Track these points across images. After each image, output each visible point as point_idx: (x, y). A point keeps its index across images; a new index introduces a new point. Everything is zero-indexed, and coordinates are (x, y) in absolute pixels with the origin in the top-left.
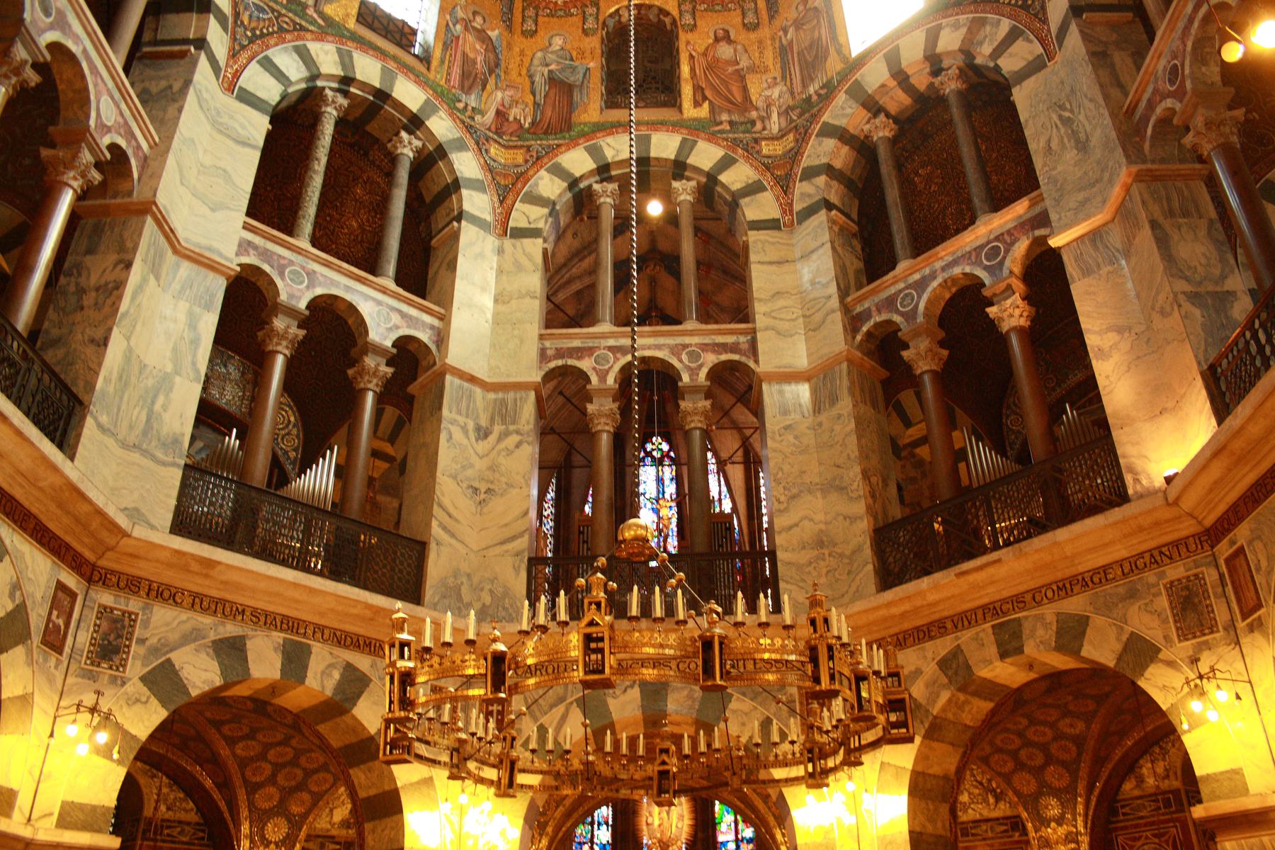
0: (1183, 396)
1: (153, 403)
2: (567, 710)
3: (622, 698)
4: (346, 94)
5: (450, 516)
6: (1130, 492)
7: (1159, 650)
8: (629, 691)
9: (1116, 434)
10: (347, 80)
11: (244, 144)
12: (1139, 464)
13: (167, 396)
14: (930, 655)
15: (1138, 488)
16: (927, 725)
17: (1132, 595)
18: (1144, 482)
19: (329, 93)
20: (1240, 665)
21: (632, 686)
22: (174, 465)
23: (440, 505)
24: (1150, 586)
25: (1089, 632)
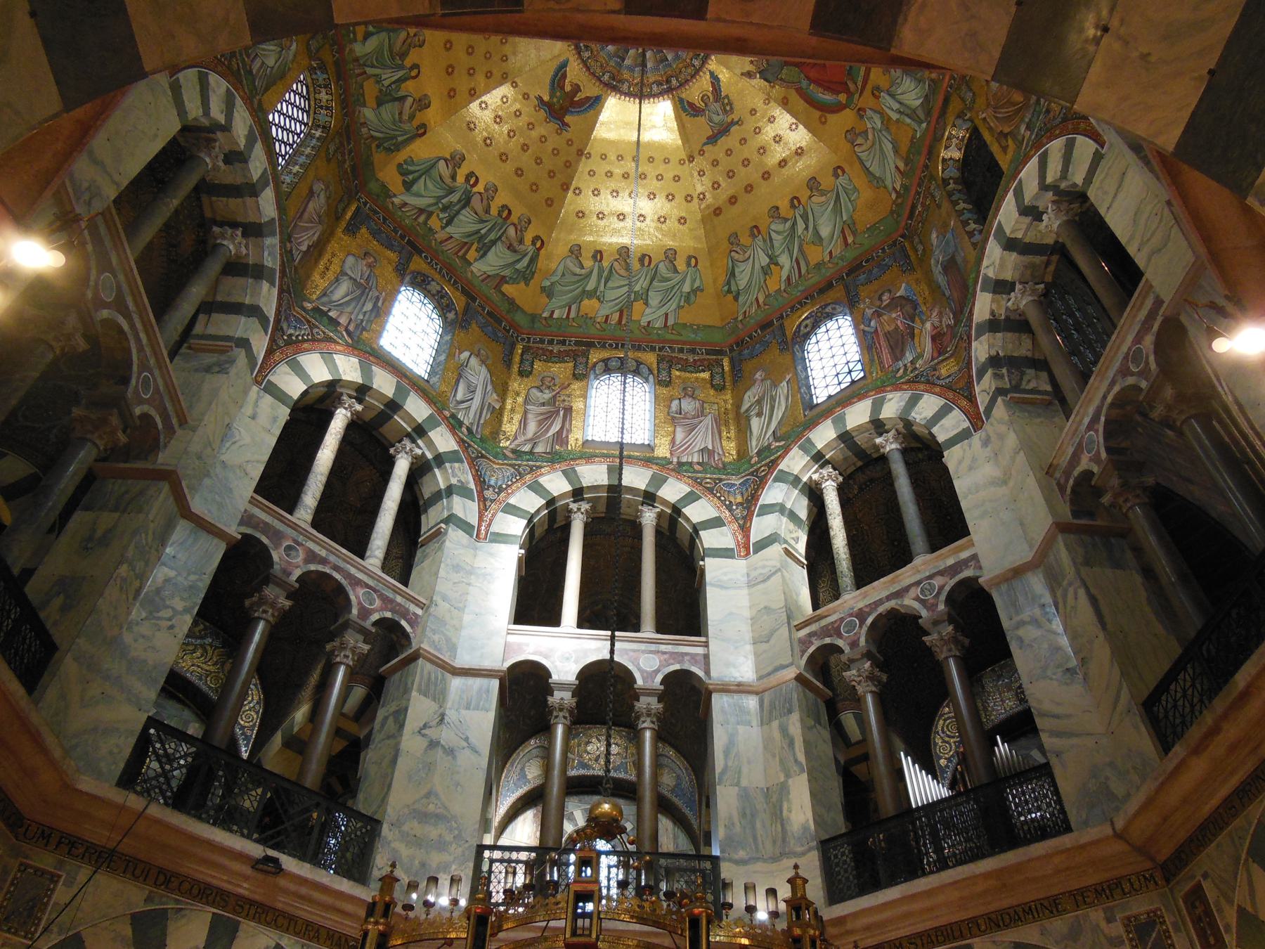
1: (781, 812)
2: (1248, 871)
4: (827, 462)
5: (1057, 717)
10: (819, 458)
11: (769, 578)
13: (788, 800)
19: (815, 477)
22: (810, 850)
23: (1044, 715)
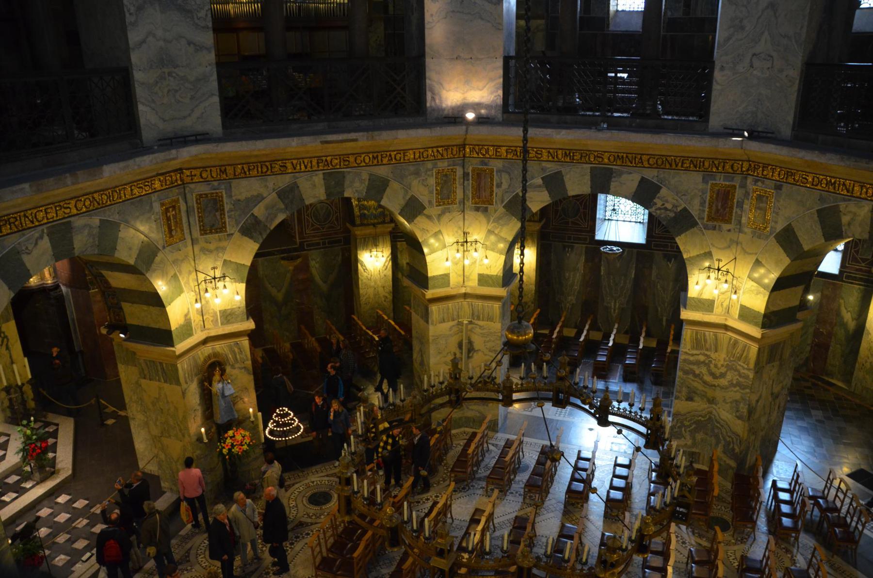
0: (477, 59)
3: (35, 253)
6: (428, 105)
7: (425, 208)
8: (40, 243)
9: (428, 60)
12: (437, 87)
14: (271, 185)
15: (433, 104)
16: (265, 236)
17: (417, 173)
18: (437, 101)
20: (461, 223)
21: (41, 237)
24: (428, 170)
25: (388, 190)
